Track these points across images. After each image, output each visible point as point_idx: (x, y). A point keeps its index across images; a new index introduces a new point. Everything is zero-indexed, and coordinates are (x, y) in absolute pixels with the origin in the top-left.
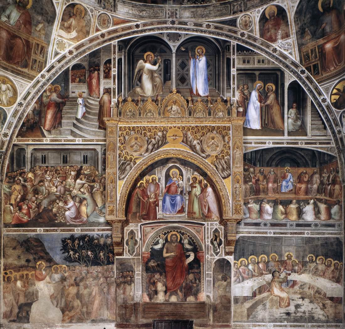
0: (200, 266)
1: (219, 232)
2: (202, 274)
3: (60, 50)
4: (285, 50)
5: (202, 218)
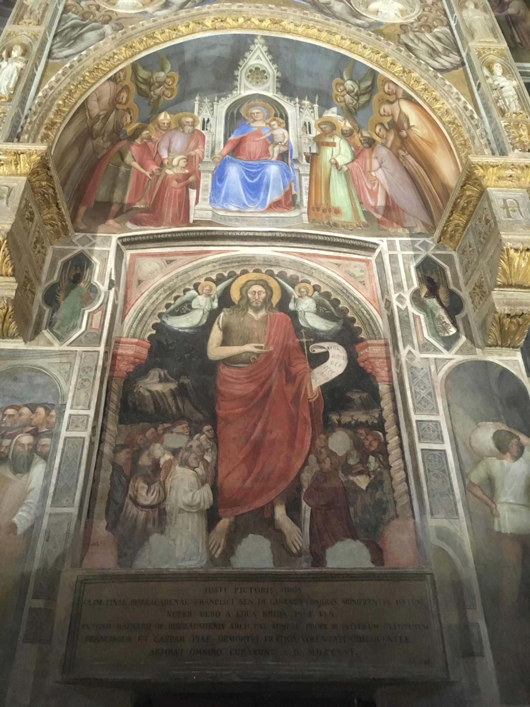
0: (375, 398)
1: (443, 270)
2: (391, 429)
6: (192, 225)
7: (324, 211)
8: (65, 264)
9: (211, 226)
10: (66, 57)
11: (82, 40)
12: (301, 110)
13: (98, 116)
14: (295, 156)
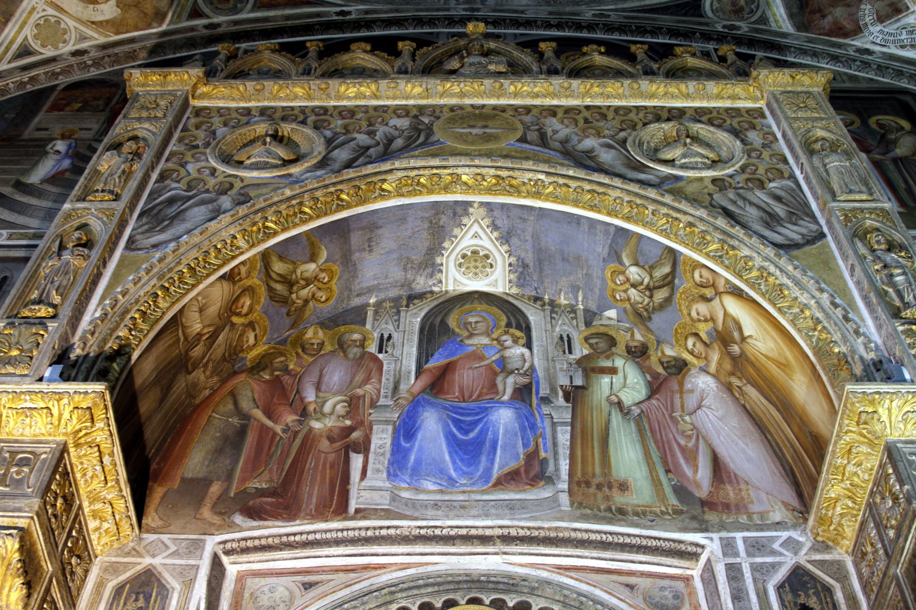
1: (828, 590)
3: (43, 46)
4: (902, 47)
5: (677, 512)
6: (352, 518)
7: (599, 487)
8: (119, 591)
9: (388, 519)
10: (154, 246)
11: (184, 220)
12: (553, 315)
13: (200, 335)
14: (544, 391)
